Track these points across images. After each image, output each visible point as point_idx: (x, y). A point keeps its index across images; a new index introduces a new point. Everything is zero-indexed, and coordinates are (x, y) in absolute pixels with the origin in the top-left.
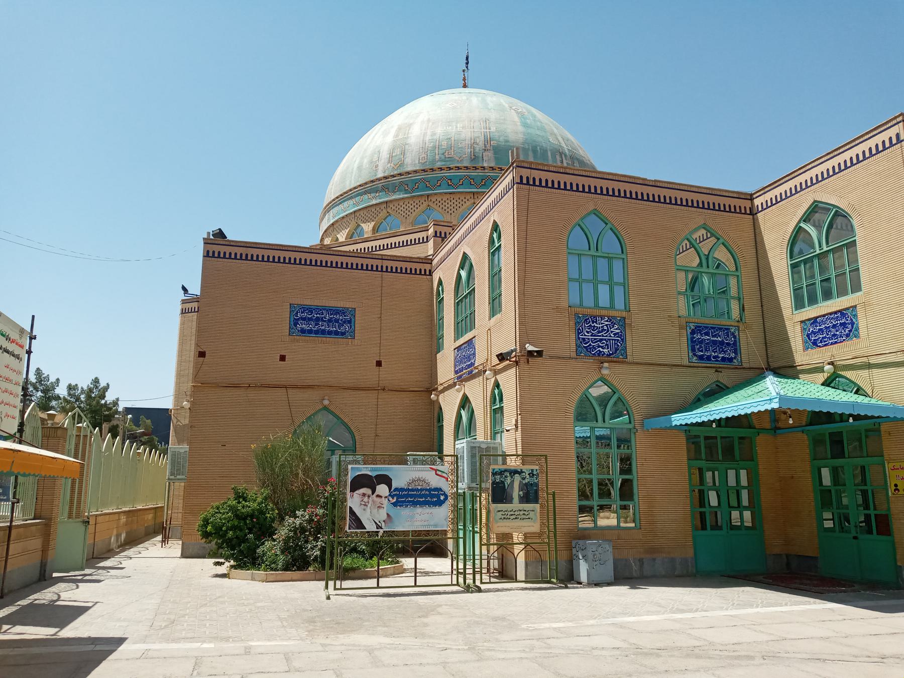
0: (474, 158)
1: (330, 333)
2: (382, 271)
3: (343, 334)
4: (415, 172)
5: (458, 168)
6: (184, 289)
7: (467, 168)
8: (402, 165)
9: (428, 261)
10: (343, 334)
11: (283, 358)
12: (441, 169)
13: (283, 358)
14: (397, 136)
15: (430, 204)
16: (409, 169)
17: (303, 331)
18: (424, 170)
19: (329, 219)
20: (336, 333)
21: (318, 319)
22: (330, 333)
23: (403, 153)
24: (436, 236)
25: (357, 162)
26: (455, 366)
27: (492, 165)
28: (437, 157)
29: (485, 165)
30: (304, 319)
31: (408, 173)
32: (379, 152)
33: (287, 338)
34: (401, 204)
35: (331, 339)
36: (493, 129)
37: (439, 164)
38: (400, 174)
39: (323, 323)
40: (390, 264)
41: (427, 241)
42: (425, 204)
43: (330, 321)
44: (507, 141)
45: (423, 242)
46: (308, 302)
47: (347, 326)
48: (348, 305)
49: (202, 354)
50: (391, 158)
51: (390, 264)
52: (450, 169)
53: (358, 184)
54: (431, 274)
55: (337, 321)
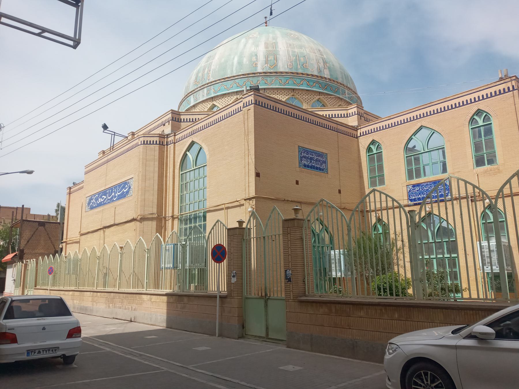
0: (320, 71)
1: (317, 168)
2: (337, 131)
3: (323, 170)
4: (287, 73)
5: (313, 75)
6: (105, 127)
7: (317, 76)
8: (276, 66)
9: (356, 129)
10: (323, 170)
11: (297, 182)
12: (303, 74)
13: (297, 182)
14: (266, 47)
15: (295, 94)
16: (282, 70)
17: (305, 166)
18: (292, 73)
19: (208, 94)
20: (320, 169)
21: (311, 159)
22: (317, 168)
23: (276, 59)
24: (358, 114)
25: (236, 59)
26: (409, 196)
27: (329, 77)
28: (299, 67)
29: (326, 76)
30: (305, 157)
31: (282, 73)
32: (256, 55)
33: (298, 169)
34: (276, 91)
35: (318, 172)
36: (325, 57)
37: (300, 71)
38: (276, 73)
39: (313, 161)
40: (340, 127)
41: (347, 117)
42: (292, 94)
43: (316, 160)
44: (333, 65)
45: (344, 117)
46: (306, 146)
47: (324, 165)
48: (324, 151)
49: (258, 175)
50: (267, 62)
51: (340, 127)
52: (308, 75)
53: (240, 74)
54: (357, 137)
55: (320, 161)
